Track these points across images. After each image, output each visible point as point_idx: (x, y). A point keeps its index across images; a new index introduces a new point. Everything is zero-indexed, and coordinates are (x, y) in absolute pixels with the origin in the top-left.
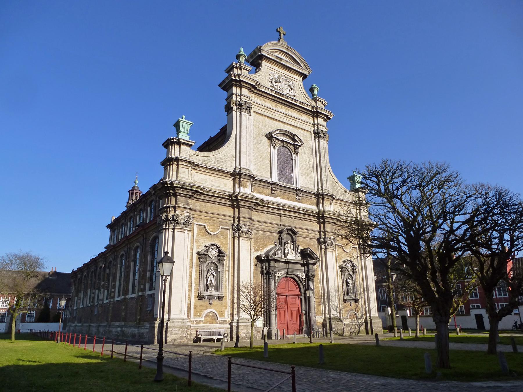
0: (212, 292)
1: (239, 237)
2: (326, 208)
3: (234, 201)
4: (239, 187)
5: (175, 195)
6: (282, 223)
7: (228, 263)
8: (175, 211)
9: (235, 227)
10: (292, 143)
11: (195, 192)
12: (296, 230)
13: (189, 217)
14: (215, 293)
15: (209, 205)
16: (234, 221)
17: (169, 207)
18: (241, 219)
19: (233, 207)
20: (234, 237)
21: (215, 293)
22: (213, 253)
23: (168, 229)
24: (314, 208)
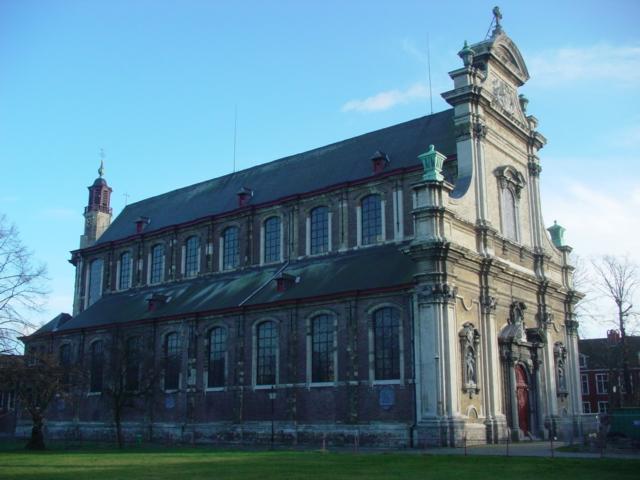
0: (471, 384)
1: (488, 314)
2: (546, 275)
3: (485, 267)
4: (485, 246)
5: (444, 259)
6: (514, 294)
7: (480, 348)
8: (445, 280)
9: (484, 301)
10: (515, 183)
11: (462, 254)
12: (526, 304)
13: (456, 288)
14: (474, 386)
15: (463, 271)
16: (481, 292)
17: (439, 275)
18: (490, 290)
19: (480, 274)
20: (483, 313)
21: (474, 386)
22: (471, 335)
23: (439, 304)
24: (531, 272)
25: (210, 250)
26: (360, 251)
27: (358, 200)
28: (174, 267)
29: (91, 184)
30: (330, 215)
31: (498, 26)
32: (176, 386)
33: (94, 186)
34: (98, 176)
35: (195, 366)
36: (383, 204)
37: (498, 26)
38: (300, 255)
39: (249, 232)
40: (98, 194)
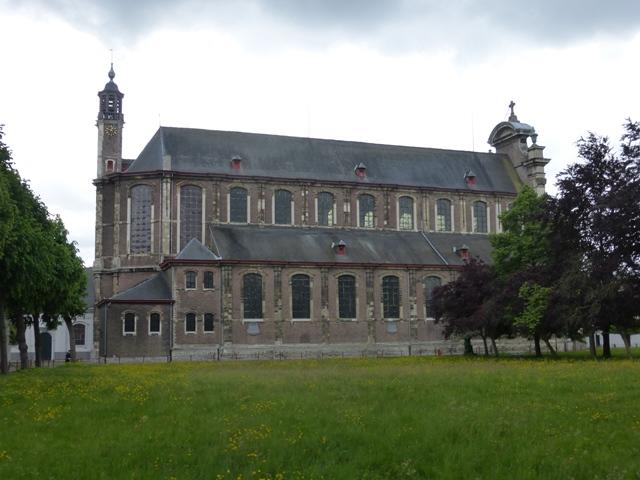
25: (347, 208)
26: (474, 235)
27: (472, 202)
28: (307, 215)
29: (102, 88)
30: (452, 207)
31: (512, 113)
32: (397, 315)
33: (104, 91)
34: (108, 80)
35: (416, 302)
36: (488, 209)
37: (512, 113)
38: (431, 229)
39: (387, 204)
40: (111, 102)
